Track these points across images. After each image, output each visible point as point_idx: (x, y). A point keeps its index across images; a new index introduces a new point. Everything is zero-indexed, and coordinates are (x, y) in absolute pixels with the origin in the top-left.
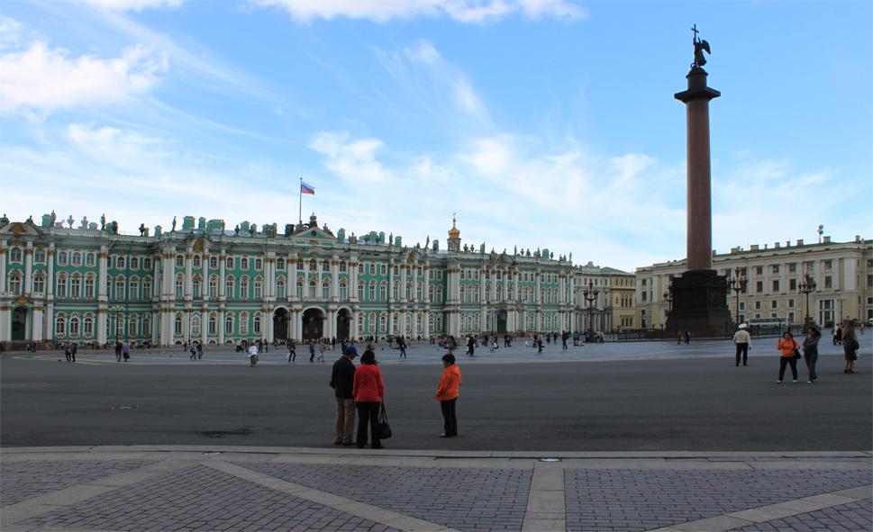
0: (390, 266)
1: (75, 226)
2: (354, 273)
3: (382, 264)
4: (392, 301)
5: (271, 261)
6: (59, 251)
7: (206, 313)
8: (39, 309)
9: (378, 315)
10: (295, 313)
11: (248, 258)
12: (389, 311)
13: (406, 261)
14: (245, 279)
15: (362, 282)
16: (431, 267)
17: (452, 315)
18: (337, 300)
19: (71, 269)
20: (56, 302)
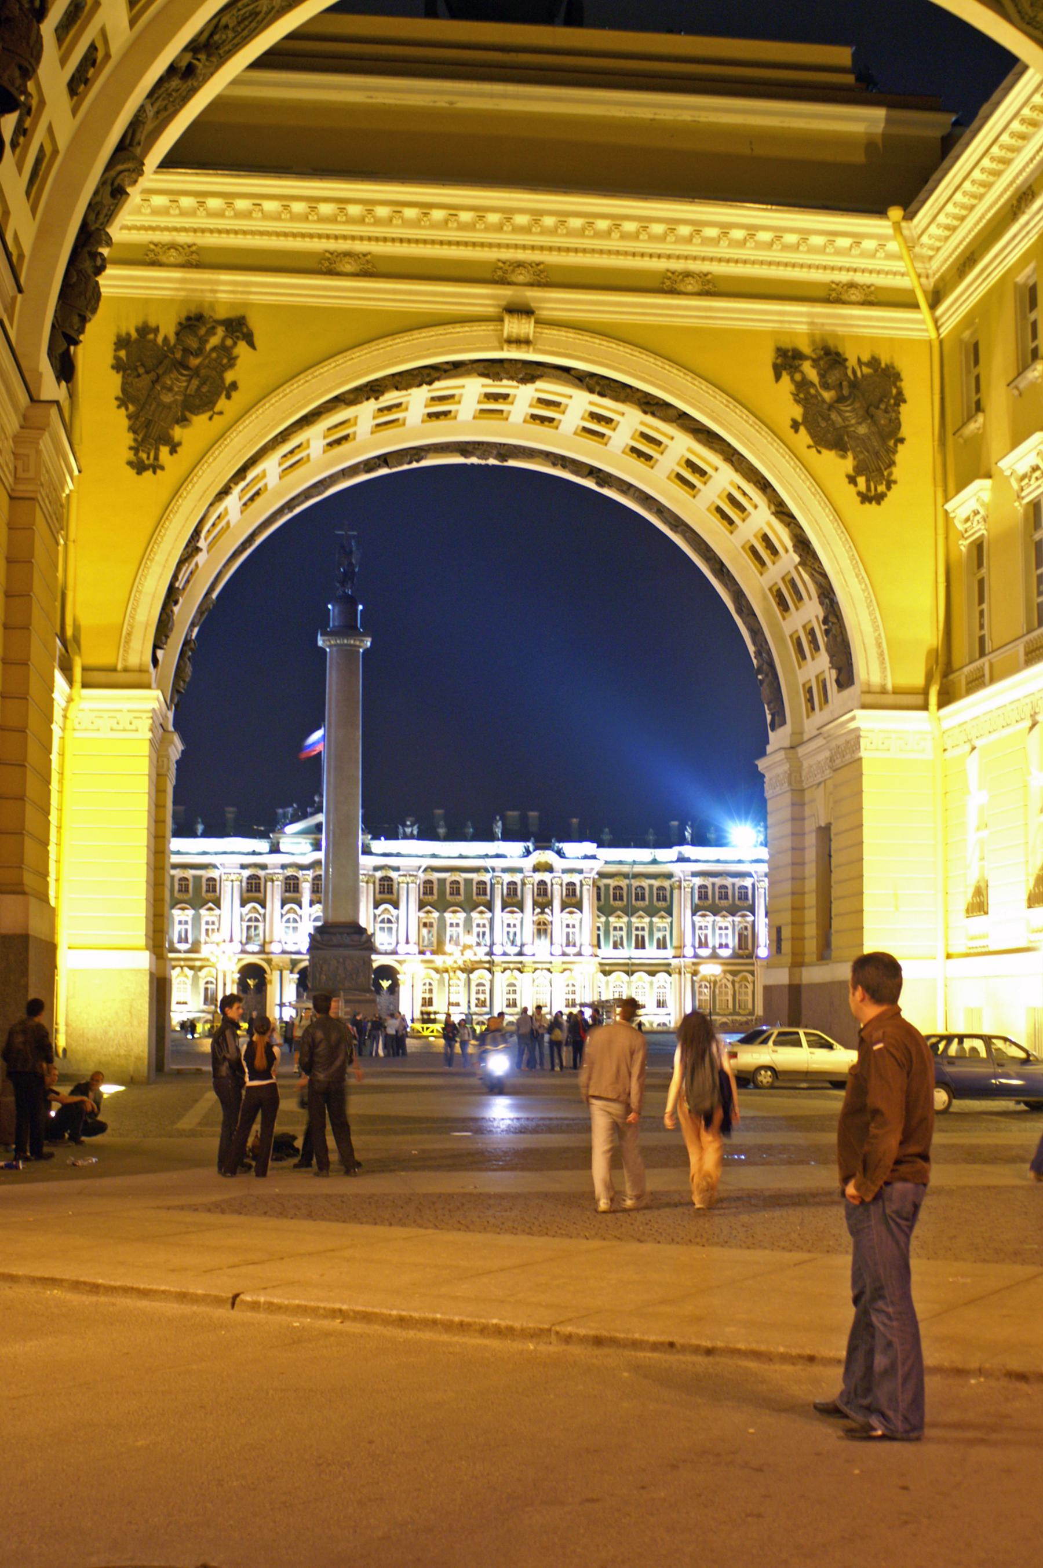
10: (276, 975)
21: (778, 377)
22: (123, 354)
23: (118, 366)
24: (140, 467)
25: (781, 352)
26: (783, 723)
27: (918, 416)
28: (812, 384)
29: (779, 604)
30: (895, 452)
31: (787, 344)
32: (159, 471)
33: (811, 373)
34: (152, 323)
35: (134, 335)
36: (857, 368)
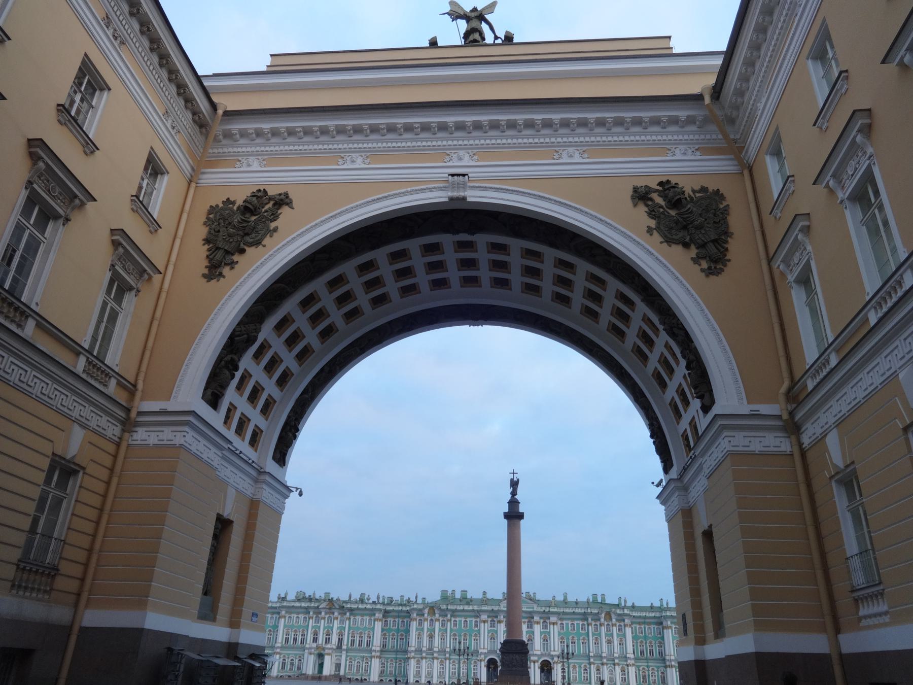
0: (588, 625)
1: (371, 601)
2: (555, 631)
3: (581, 623)
4: (591, 654)
5: (484, 622)
6: (352, 618)
7: (435, 661)
8: (328, 654)
9: (580, 667)
11: (468, 620)
12: (590, 664)
13: (602, 620)
14: (465, 635)
15: (562, 638)
16: (632, 623)
17: (668, 669)
18: (539, 653)
19: (358, 628)
20: (347, 650)
21: (635, 205)
22: (211, 216)
23: (208, 222)
24: (209, 277)
25: (635, 190)
26: (672, 465)
27: (739, 221)
28: (661, 207)
29: (659, 384)
30: (726, 242)
31: (641, 183)
32: (222, 279)
33: (659, 200)
34: (232, 199)
35: (221, 205)
36: (691, 193)
